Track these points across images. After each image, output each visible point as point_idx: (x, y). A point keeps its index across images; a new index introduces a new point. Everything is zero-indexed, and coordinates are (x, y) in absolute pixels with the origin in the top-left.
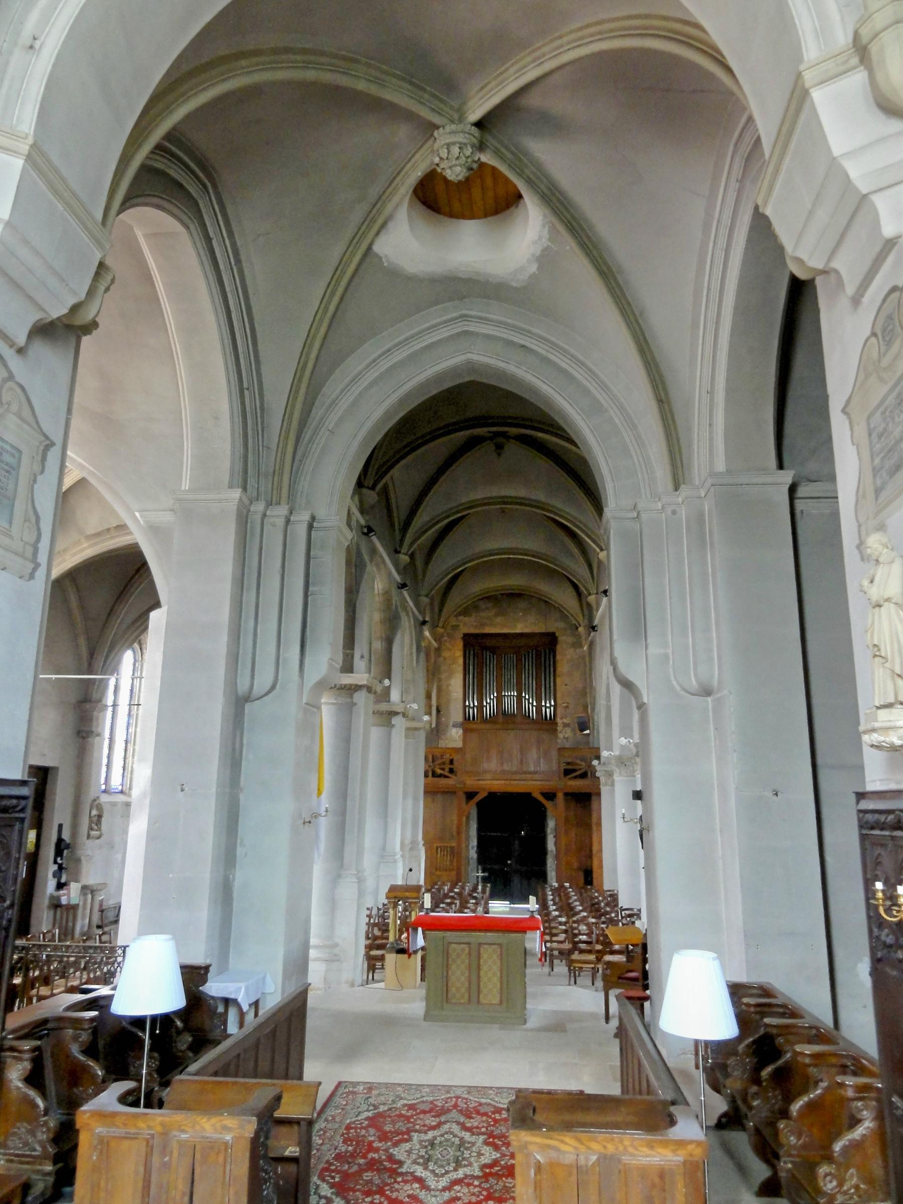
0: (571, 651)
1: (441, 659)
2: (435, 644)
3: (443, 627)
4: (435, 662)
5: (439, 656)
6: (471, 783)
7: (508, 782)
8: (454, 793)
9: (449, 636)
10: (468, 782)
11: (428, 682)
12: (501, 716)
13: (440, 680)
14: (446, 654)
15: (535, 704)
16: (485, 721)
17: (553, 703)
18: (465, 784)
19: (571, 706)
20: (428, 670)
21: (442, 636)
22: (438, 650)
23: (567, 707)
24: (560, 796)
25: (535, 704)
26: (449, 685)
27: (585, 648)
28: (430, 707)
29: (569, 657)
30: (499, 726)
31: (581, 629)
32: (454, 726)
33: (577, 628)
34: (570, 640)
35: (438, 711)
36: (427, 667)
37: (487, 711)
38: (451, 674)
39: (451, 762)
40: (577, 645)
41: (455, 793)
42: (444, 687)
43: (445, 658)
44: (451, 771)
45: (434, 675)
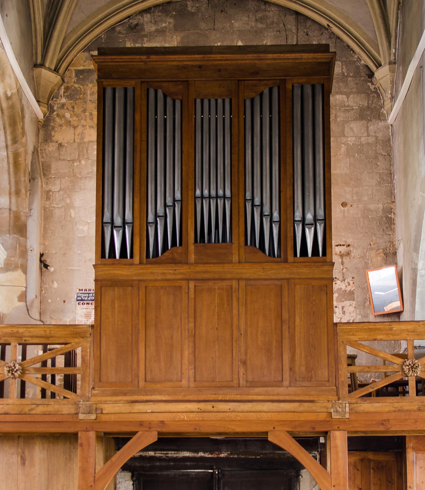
0: (356, 127)
1: (51, 148)
2: (39, 112)
3: (56, 70)
4: (35, 151)
5: (48, 139)
6: (116, 410)
7: (208, 406)
8: (71, 438)
9: (72, 94)
10: (108, 408)
11: (18, 193)
12: (192, 247)
13: (48, 195)
14: (62, 135)
15: (276, 215)
16: (152, 257)
17: (321, 213)
18: (99, 411)
19: (355, 253)
20: (16, 164)
21: (53, 95)
22: (45, 127)
23: (348, 254)
24: (339, 442)
25: (276, 215)
26: (68, 207)
27: (391, 119)
28: (24, 253)
29: (351, 140)
30: (184, 269)
31: (382, 74)
32: (80, 300)
33: (371, 75)
34: (355, 101)
35: (44, 265)
36: (16, 155)
37: (157, 234)
38: (75, 179)
39: (70, 360)
40: (373, 112)
41: (71, 438)
42: (57, 213)
43: (60, 145)
44: (70, 384)
45: (32, 179)
